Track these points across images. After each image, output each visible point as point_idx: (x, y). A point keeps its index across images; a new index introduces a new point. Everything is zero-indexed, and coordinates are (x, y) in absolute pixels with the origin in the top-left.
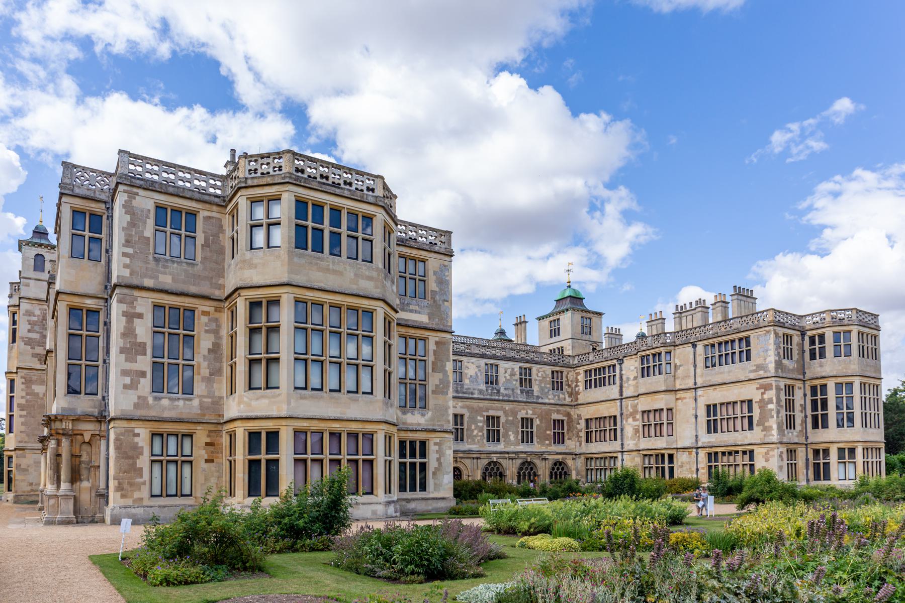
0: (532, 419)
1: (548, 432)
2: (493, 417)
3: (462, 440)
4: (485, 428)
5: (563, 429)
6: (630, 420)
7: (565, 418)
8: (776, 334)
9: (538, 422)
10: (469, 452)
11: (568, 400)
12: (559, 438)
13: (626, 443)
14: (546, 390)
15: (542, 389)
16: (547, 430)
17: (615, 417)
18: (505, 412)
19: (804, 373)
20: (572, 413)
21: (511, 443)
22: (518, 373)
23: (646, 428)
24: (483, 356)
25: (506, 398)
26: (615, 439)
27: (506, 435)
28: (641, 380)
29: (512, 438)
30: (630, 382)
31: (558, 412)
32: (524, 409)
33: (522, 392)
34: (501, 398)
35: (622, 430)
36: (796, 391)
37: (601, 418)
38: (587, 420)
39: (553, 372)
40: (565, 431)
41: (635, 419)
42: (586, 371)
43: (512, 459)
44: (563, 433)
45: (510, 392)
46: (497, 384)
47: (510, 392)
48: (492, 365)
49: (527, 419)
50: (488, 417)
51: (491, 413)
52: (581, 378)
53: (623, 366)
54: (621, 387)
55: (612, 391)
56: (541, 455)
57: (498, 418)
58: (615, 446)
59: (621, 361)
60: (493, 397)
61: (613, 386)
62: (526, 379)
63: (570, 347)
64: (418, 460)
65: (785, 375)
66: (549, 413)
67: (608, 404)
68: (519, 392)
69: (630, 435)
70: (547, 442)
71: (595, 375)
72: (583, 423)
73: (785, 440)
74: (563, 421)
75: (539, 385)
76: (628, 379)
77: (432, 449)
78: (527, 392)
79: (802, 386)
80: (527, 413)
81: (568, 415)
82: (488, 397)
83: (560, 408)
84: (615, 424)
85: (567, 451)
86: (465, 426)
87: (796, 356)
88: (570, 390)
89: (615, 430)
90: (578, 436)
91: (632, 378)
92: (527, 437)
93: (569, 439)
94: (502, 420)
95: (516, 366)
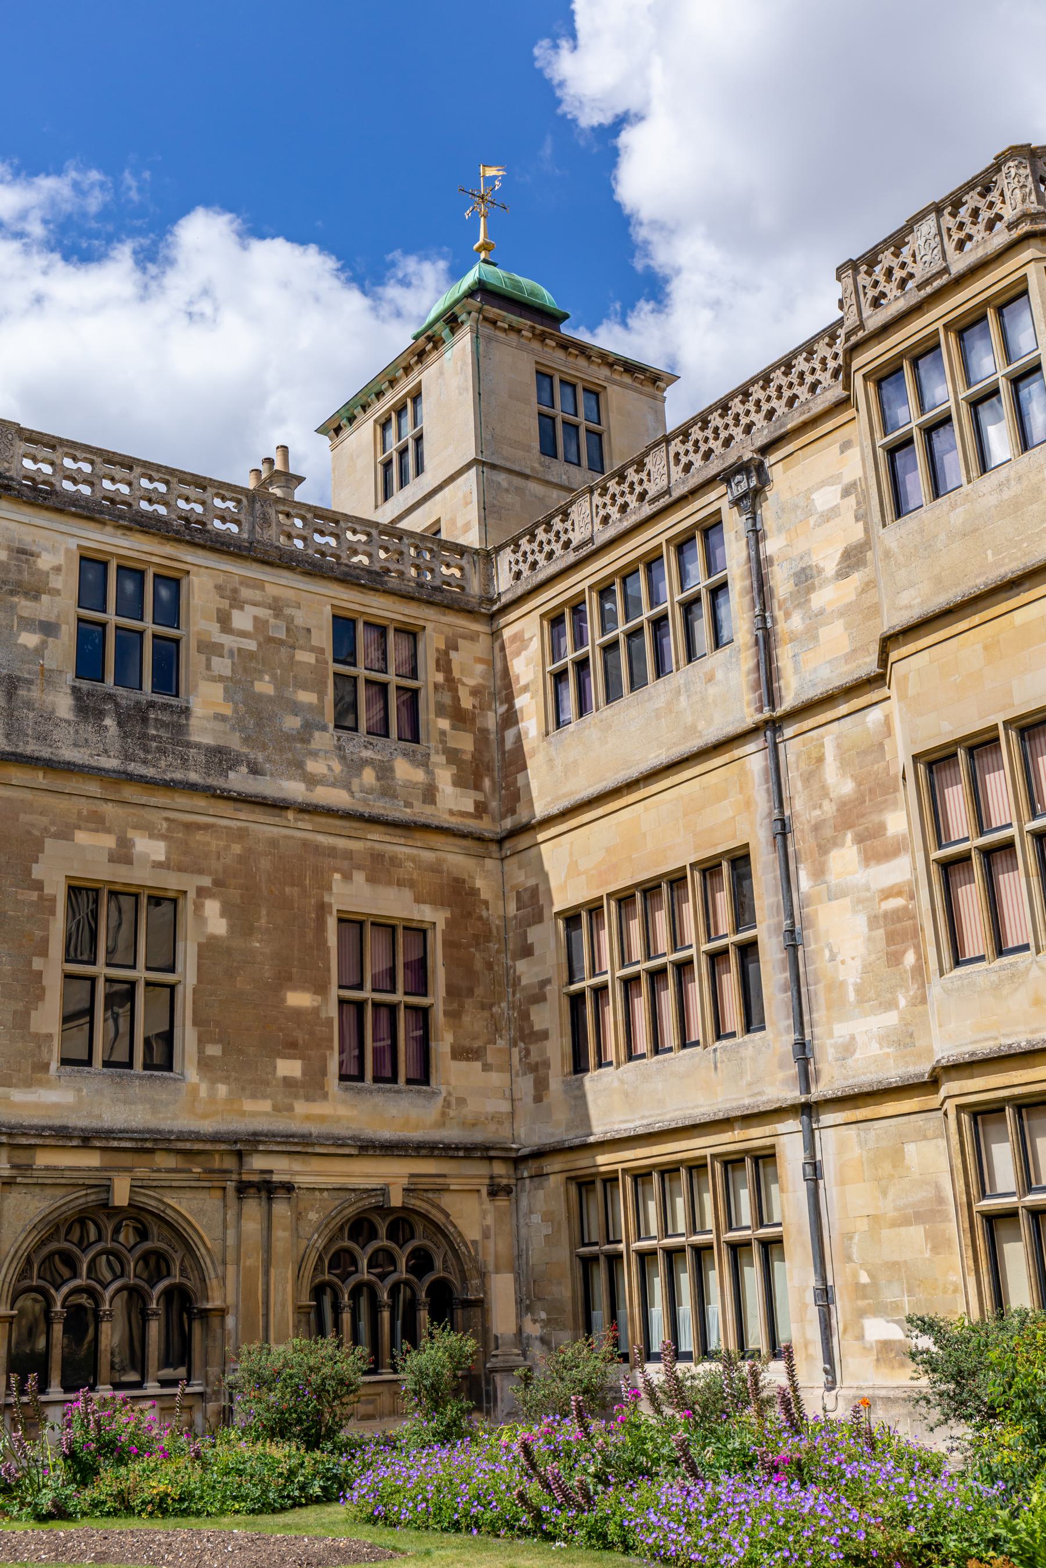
1: (298, 999)
5: (420, 984)
6: (845, 859)
9: (214, 920)
11: (453, 801)
12: (386, 1046)
13: (830, 1034)
14: (292, 723)
15: (254, 715)
16: (285, 980)
17: (740, 860)
20: (484, 885)
23: (971, 897)
26: (752, 1020)
28: (894, 537)
30: (824, 597)
31: (380, 869)
32: (97, 823)
35: (793, 942)
37: (650, 889)
38: (572, 919)
39: (344, 626)
41: (876, 848)
42: (556, 621)
44: (422, 1014)
52: (528, 665)
53: (768, 511)
54: (766, 642)
55: (714, 691)
58: (750, 1072)
59: (750, 482)
61: (713, 661)
62: (130, 640)
63: (472, 513)
66: (308, 869)
67: (688, 787)
69: (850, 974)
70: (290, 1068)
71: (607, 621)
72: (547, 938)
75: (237, 686)
76: (806, 579)
78: (133, 719)
80: (123, 855)
81: (459, 895)
83: (399, 847)
84: (743, 912)
85: (452, 1134)
88: (465, 743)
89: (748, 950)
90: (529, 1036)
91: (831, 566)
93: (460, 1053)
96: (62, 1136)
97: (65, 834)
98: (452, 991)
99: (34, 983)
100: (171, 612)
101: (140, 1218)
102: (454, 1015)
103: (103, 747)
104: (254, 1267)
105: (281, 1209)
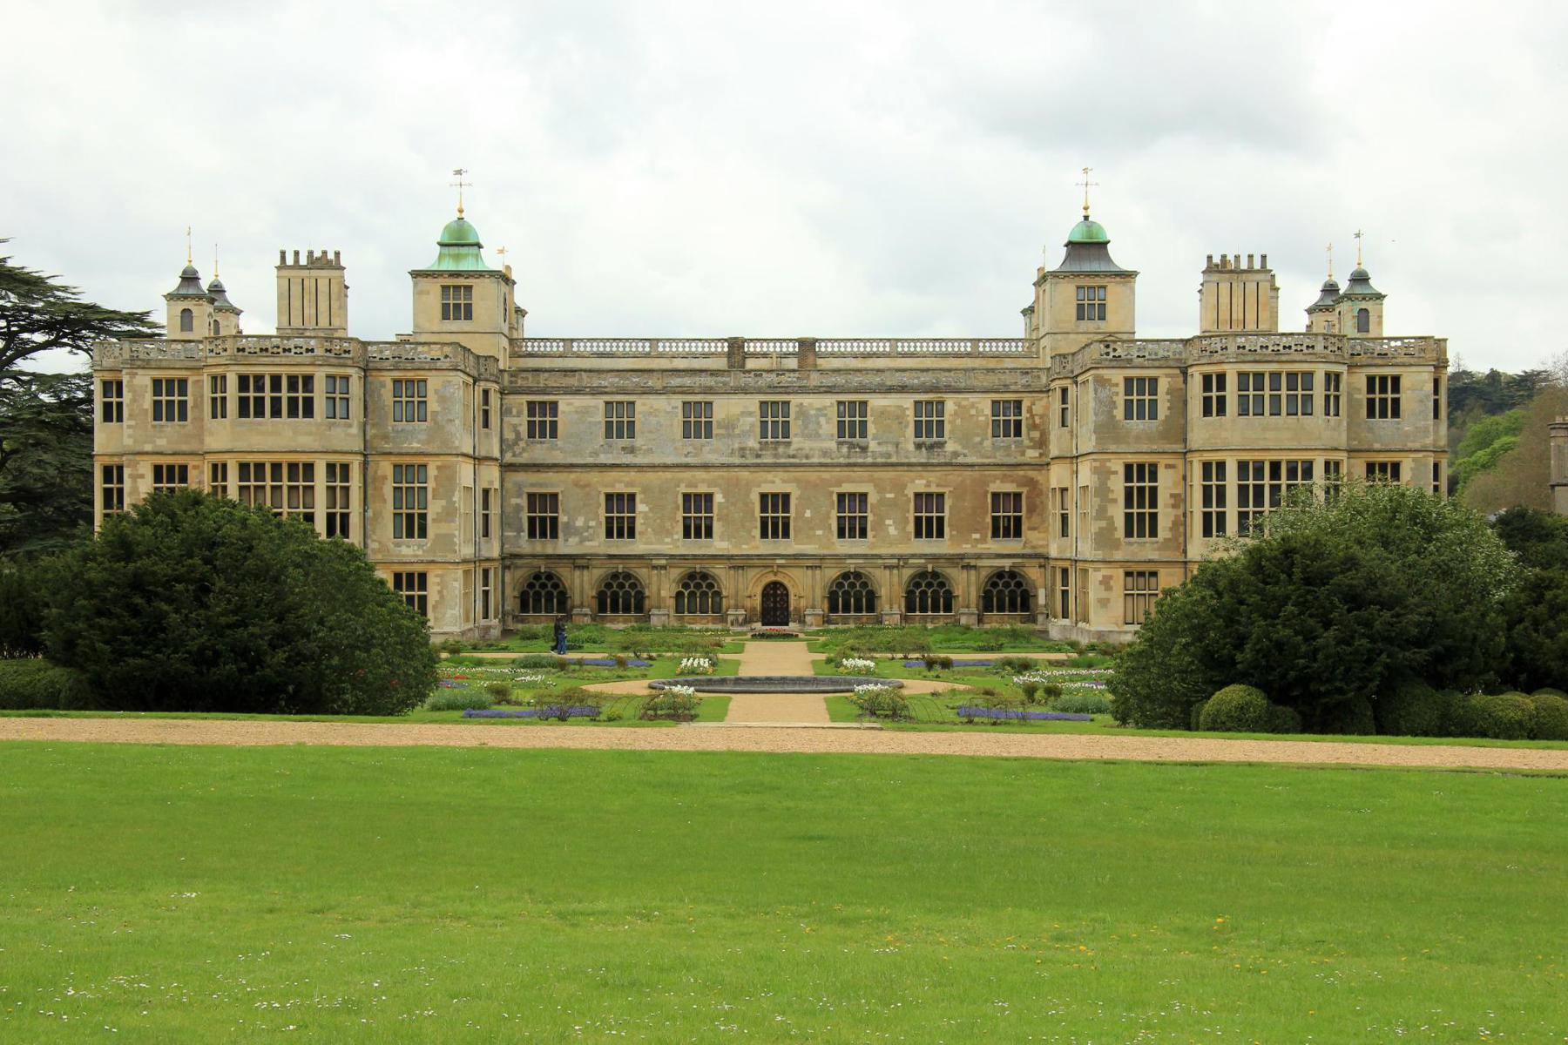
0: (941, 496)
2: (852, 495)
3: (786, 534)
4: (834, 514)
7: (1024, 490)
8: (1101, 382)
10: (796, 557)
11: (1032, 454)
18: (880, 489)
19: (1185, 441)
20: (1040, 478)
21: (892, 538)
22: (910, 412)
24: (830, 390)
25: (879, 460)
27: (880, 525)
29: (892, 531)
31: (1004, 479)
32: (922, 478)
33: (919, 446)
34: (869, 460)
36: (1161, 472)
40: (1023, 513)
43: (890, 567)
45: (890, 448)
46: (864, 434)
47: (890, 448)
48: (852, 403)
49: (929, 495)
50: (841, 496)
51: (847, 488)
56: (957, 560)
57: (864, 496)
60: (852, 461)
64: (416, 593)
65: (1123, 448)
68: (911, 447)
70: (977, 536)
73: (1118, 555)
74: (1018, 496)
77: (431, 580)
79: (1179, 462)
81: (1032, 483)
82: (842, 460)
85: (1028, 551)
86: (792, 514)
87: (1163, 410)
92: (929, 527)
94: (872, 499)
95: (907, 401)
96: (914, 556)
97: (913, 481)
98: (1031, 510)
99: (907, 522)
100: (941, 413)
101: (935, 575)
102: (1028, 519)
103: (922, 457)
104: (966, 587)
105: (973, 572)
